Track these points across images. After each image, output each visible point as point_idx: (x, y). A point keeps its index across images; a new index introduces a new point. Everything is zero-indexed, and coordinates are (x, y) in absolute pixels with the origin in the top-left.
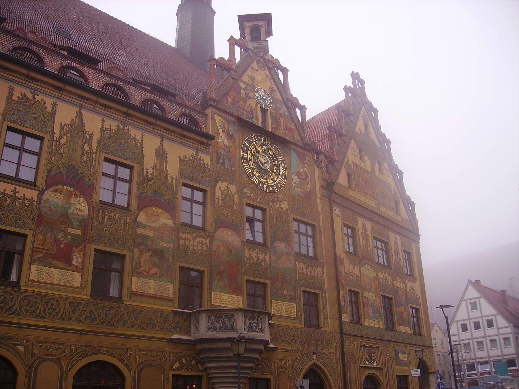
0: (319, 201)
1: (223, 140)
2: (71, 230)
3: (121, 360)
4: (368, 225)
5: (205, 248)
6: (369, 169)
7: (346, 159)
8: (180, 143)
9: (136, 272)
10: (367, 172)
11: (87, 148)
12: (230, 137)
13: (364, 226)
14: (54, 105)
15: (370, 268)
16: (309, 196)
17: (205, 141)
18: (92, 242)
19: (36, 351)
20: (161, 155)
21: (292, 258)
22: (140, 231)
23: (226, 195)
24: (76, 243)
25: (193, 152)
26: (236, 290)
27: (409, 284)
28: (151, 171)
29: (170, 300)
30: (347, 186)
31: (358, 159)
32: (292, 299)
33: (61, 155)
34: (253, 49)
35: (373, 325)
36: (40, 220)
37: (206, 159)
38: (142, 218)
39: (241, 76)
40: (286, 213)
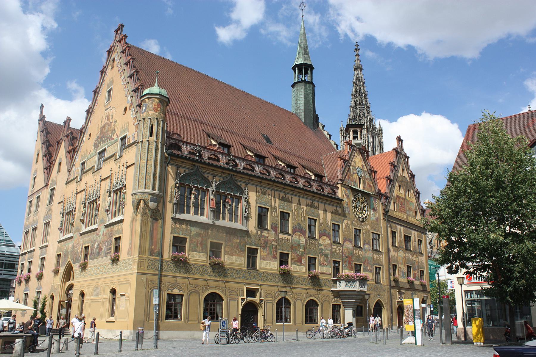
1: (345, 199)
2: (301, 250)
4: (402, 228)
6: (404, 197)
8: (331, 205)
9: (320, 264)
10: (402, 198)
12: (348, 197)
13: (400, 230)
14: (292, 198)
16: (377, 220)
17: (339, 202)
18: (307, 254)
21: (371, 252)
22: (320, 247)
23: (347, 226)
24: (303, 254)
25: (335, 208)
26: (351, 269)
27: (420, 258)
29: (330, 274)
32: (371, 271)
36: (292, 247)
40: (369, 230)
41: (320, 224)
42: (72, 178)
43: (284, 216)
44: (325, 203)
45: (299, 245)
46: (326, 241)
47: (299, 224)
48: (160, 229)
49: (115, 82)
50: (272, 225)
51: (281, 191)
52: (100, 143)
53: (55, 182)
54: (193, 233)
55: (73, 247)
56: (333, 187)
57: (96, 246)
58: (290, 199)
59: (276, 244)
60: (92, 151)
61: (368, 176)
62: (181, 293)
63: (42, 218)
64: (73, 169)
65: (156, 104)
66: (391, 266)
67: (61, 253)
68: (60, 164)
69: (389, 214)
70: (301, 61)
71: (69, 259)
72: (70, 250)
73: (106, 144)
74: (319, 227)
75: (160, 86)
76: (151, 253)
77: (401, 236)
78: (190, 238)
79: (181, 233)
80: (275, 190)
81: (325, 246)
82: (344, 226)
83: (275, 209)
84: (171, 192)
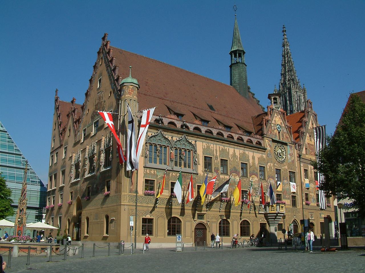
0: (296, 162)
1: (269, 148)
3: (249, 219)
5: (266, 186)
7: (305, 143)
10: (312, 145)
11: (237, 161)
12: (270, 146)
14: (229, 149)
15: (312, 184)
16: (293, 161)
19: (233, 218)
20: (253, 158)
23: (270, 167)
28: (251, 164)
30: (305, 154)
31: (309, 141)
32: (289, 199)
33: (232, 164)
34: (275, 108)
35: (313, 205)
37: (264, 156)
38: (250, 180)
39: (272, 122)
41: (250, 167)
42: (78, 140)
43: (224, 162)
44: (253, 152)
45: (235, 182)
46: (255, 179)
47: (234, 167)
48: (136, 175)
49: (103, 73)
50: (214, 169)
51: (220, 145)
52: (95, 116)
53: (67, 143)
54: (159, 176)
55: (80, 188)
56: (259, 140)
57: (95, 186)
58: (227, 150)
59: (218, 182)
60: (90, 121)
61: (285, 131)
62: (152, 217)
63: (60, 167)
64: (79, 134)
65: (130, 89)
66: (304, 195)
67: (73, 191)
68: (70, 130)
69: (302, 157)
70: (235, 48)
71: (78, 195)
72: (78, 189)
73: (99, 117)
74: (249, 169)
75: (133, 77)
76: (131, 191)
77: (311, 173)
78: (157, 180)
79: (150, 177)
80: (216, 144)
81: (254, 182)
82: (268, 167)
83: (216, 158)
84: (143, 149)
